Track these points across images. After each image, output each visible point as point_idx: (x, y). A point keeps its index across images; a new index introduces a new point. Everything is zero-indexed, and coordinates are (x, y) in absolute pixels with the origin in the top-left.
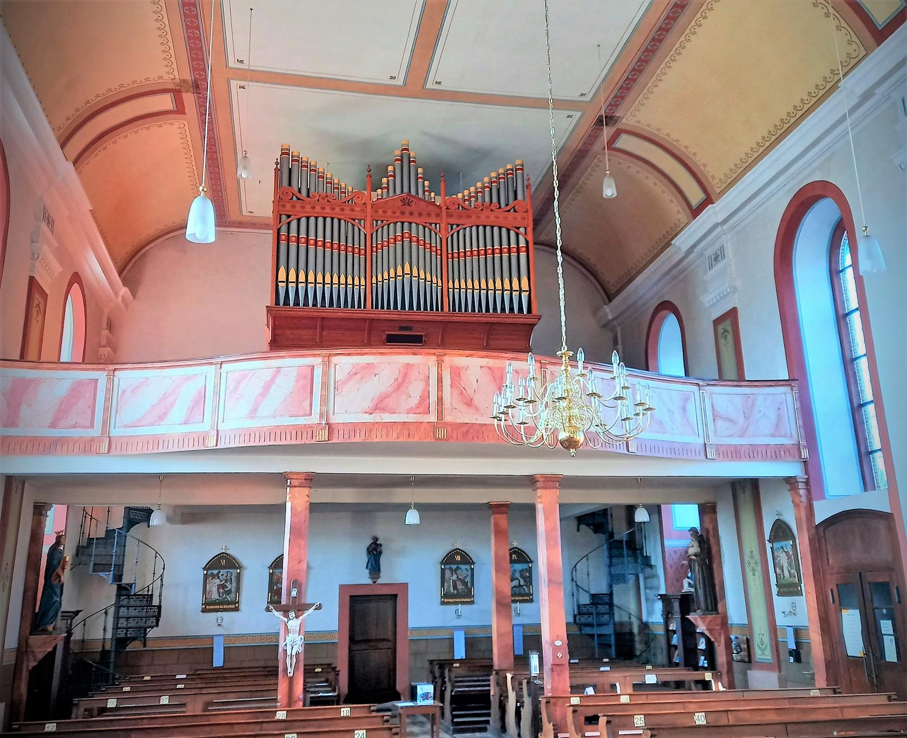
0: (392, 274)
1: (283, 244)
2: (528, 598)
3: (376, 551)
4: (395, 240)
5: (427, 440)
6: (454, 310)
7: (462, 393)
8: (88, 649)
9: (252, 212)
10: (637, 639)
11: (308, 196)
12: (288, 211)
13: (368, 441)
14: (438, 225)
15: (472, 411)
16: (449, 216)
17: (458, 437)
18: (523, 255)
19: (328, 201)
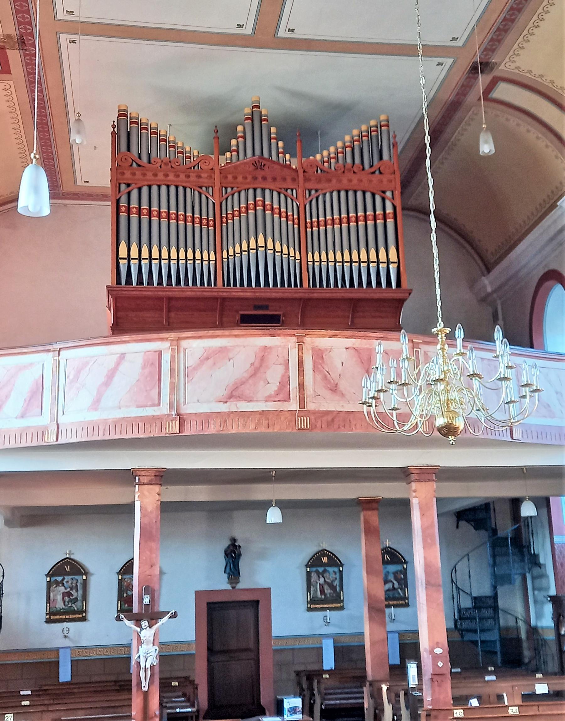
1: (123, 216)
2: (403, 602)
3: (235, 554)
4: (247, 208)
5: (288, 431)
6: (314, 285)
7: (325, 378)
9: (87, 182)
10: (525, 645)
11: (149, 162)
12: (127, 179)
13: (223, 432)
14: (294, 191)
16: (306, 180)
17: (323, 426)
18: (390, 222)
19: (171, 167)
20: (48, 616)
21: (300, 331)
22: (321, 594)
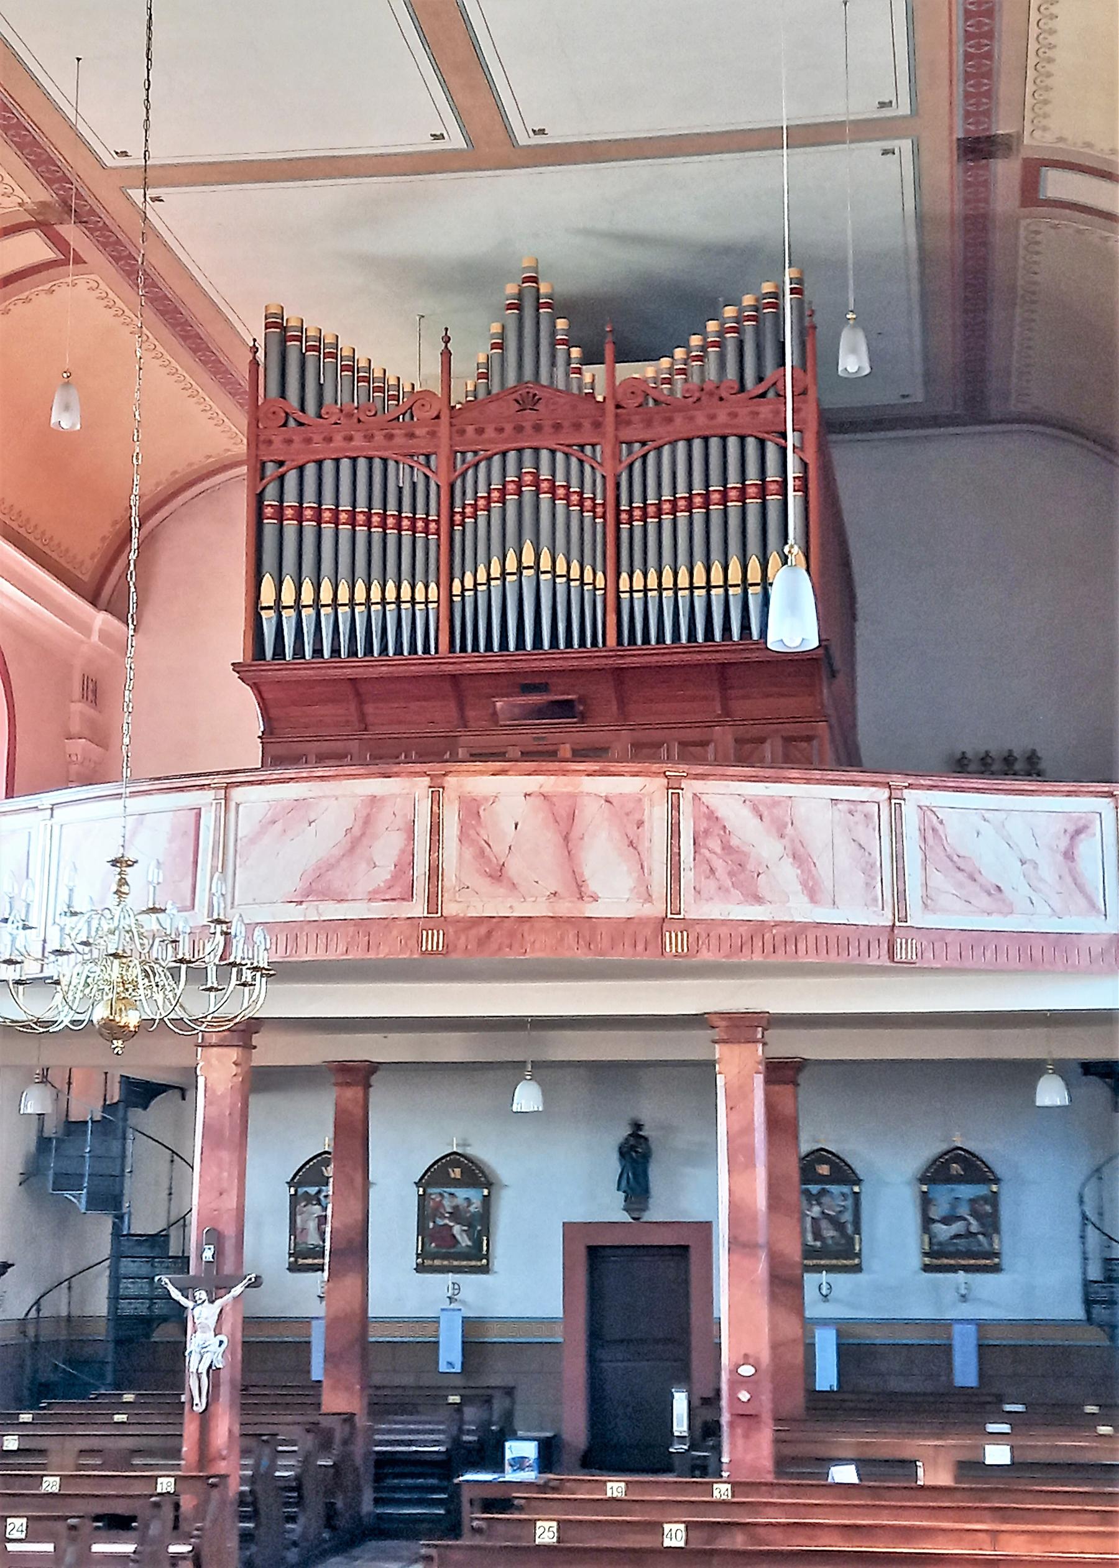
0: (496, 572)
1: (270, 525)
3: (636, 1152)
4: (503, 492)
8: (82, 1334)
14: (598, 448)
15: (502, 891)
17: (469, 947)
20: (292, 1259)
21: (436, 768)
22: (815, 1240)
